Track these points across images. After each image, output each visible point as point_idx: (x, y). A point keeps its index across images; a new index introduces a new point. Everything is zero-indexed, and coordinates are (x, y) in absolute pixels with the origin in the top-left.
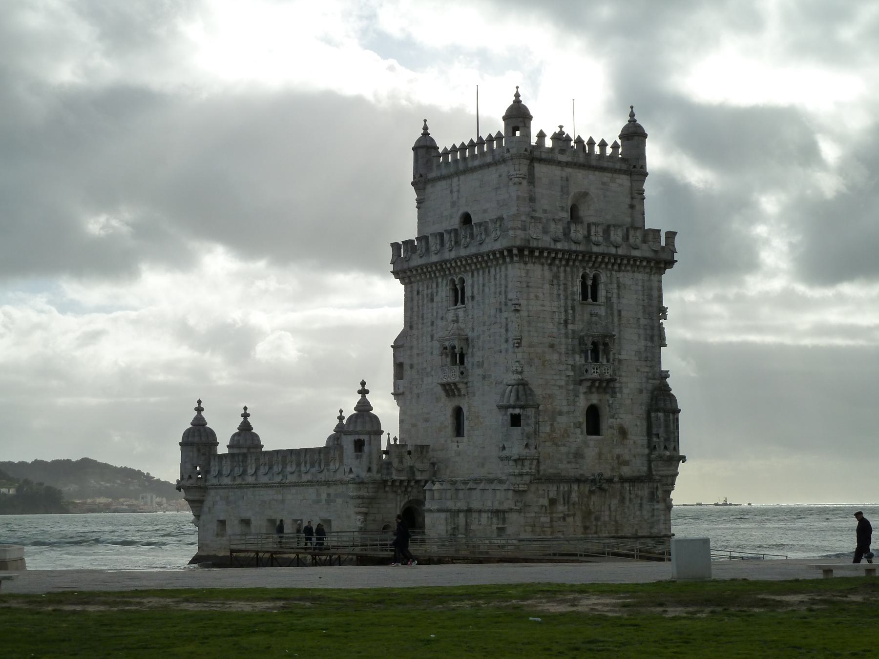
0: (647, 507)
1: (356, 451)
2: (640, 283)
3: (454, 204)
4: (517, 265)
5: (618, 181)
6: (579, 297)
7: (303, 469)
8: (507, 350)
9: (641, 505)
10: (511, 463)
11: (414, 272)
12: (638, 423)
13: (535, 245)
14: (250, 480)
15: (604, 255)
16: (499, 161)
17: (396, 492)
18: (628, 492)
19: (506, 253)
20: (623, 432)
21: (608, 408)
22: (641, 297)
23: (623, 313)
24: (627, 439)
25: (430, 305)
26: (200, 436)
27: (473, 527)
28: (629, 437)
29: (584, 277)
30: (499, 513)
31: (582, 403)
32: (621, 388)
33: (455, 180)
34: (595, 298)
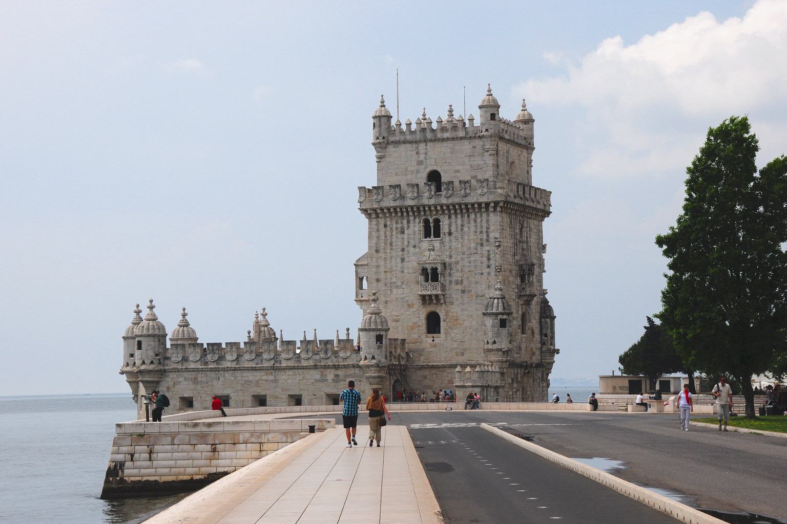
0: (541, 384)
1: (377, 343)
3: (420, 163)
4: (498, 213)
5: (523, 153)
6: (518, 237)
7: (303, 356)
8: (489, 274)
10: (500, 353)
11: (386, 211)
14: (229, 365)
16: (475, 137)
17: (390, 374)
19: (492, 205)
20: (533, 333)
23: (532, 248)
25: (400, 236)
26: (159, 329)
27: (489, 398)
30: (496, 388)
33: (422, 146)
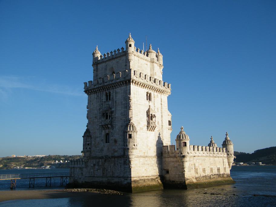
2: (123, 90)
9: (121, 166)
12: (121, 137)
13: (89, 89)
15: (108, 85)
18: (116, 162)
20: (116, 141)
21: (111, 134)
22: (123, 94)
24: (117, 143)
28: (117, 142)
29: (107, 94)
30: (81, 168)
31: (103, 133)
32: (115, 126)
34: (110, 99)
